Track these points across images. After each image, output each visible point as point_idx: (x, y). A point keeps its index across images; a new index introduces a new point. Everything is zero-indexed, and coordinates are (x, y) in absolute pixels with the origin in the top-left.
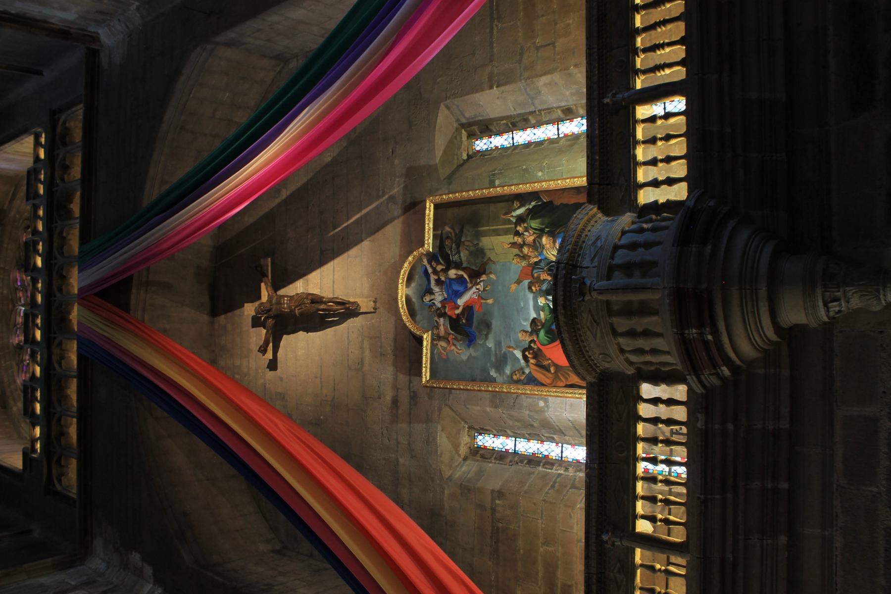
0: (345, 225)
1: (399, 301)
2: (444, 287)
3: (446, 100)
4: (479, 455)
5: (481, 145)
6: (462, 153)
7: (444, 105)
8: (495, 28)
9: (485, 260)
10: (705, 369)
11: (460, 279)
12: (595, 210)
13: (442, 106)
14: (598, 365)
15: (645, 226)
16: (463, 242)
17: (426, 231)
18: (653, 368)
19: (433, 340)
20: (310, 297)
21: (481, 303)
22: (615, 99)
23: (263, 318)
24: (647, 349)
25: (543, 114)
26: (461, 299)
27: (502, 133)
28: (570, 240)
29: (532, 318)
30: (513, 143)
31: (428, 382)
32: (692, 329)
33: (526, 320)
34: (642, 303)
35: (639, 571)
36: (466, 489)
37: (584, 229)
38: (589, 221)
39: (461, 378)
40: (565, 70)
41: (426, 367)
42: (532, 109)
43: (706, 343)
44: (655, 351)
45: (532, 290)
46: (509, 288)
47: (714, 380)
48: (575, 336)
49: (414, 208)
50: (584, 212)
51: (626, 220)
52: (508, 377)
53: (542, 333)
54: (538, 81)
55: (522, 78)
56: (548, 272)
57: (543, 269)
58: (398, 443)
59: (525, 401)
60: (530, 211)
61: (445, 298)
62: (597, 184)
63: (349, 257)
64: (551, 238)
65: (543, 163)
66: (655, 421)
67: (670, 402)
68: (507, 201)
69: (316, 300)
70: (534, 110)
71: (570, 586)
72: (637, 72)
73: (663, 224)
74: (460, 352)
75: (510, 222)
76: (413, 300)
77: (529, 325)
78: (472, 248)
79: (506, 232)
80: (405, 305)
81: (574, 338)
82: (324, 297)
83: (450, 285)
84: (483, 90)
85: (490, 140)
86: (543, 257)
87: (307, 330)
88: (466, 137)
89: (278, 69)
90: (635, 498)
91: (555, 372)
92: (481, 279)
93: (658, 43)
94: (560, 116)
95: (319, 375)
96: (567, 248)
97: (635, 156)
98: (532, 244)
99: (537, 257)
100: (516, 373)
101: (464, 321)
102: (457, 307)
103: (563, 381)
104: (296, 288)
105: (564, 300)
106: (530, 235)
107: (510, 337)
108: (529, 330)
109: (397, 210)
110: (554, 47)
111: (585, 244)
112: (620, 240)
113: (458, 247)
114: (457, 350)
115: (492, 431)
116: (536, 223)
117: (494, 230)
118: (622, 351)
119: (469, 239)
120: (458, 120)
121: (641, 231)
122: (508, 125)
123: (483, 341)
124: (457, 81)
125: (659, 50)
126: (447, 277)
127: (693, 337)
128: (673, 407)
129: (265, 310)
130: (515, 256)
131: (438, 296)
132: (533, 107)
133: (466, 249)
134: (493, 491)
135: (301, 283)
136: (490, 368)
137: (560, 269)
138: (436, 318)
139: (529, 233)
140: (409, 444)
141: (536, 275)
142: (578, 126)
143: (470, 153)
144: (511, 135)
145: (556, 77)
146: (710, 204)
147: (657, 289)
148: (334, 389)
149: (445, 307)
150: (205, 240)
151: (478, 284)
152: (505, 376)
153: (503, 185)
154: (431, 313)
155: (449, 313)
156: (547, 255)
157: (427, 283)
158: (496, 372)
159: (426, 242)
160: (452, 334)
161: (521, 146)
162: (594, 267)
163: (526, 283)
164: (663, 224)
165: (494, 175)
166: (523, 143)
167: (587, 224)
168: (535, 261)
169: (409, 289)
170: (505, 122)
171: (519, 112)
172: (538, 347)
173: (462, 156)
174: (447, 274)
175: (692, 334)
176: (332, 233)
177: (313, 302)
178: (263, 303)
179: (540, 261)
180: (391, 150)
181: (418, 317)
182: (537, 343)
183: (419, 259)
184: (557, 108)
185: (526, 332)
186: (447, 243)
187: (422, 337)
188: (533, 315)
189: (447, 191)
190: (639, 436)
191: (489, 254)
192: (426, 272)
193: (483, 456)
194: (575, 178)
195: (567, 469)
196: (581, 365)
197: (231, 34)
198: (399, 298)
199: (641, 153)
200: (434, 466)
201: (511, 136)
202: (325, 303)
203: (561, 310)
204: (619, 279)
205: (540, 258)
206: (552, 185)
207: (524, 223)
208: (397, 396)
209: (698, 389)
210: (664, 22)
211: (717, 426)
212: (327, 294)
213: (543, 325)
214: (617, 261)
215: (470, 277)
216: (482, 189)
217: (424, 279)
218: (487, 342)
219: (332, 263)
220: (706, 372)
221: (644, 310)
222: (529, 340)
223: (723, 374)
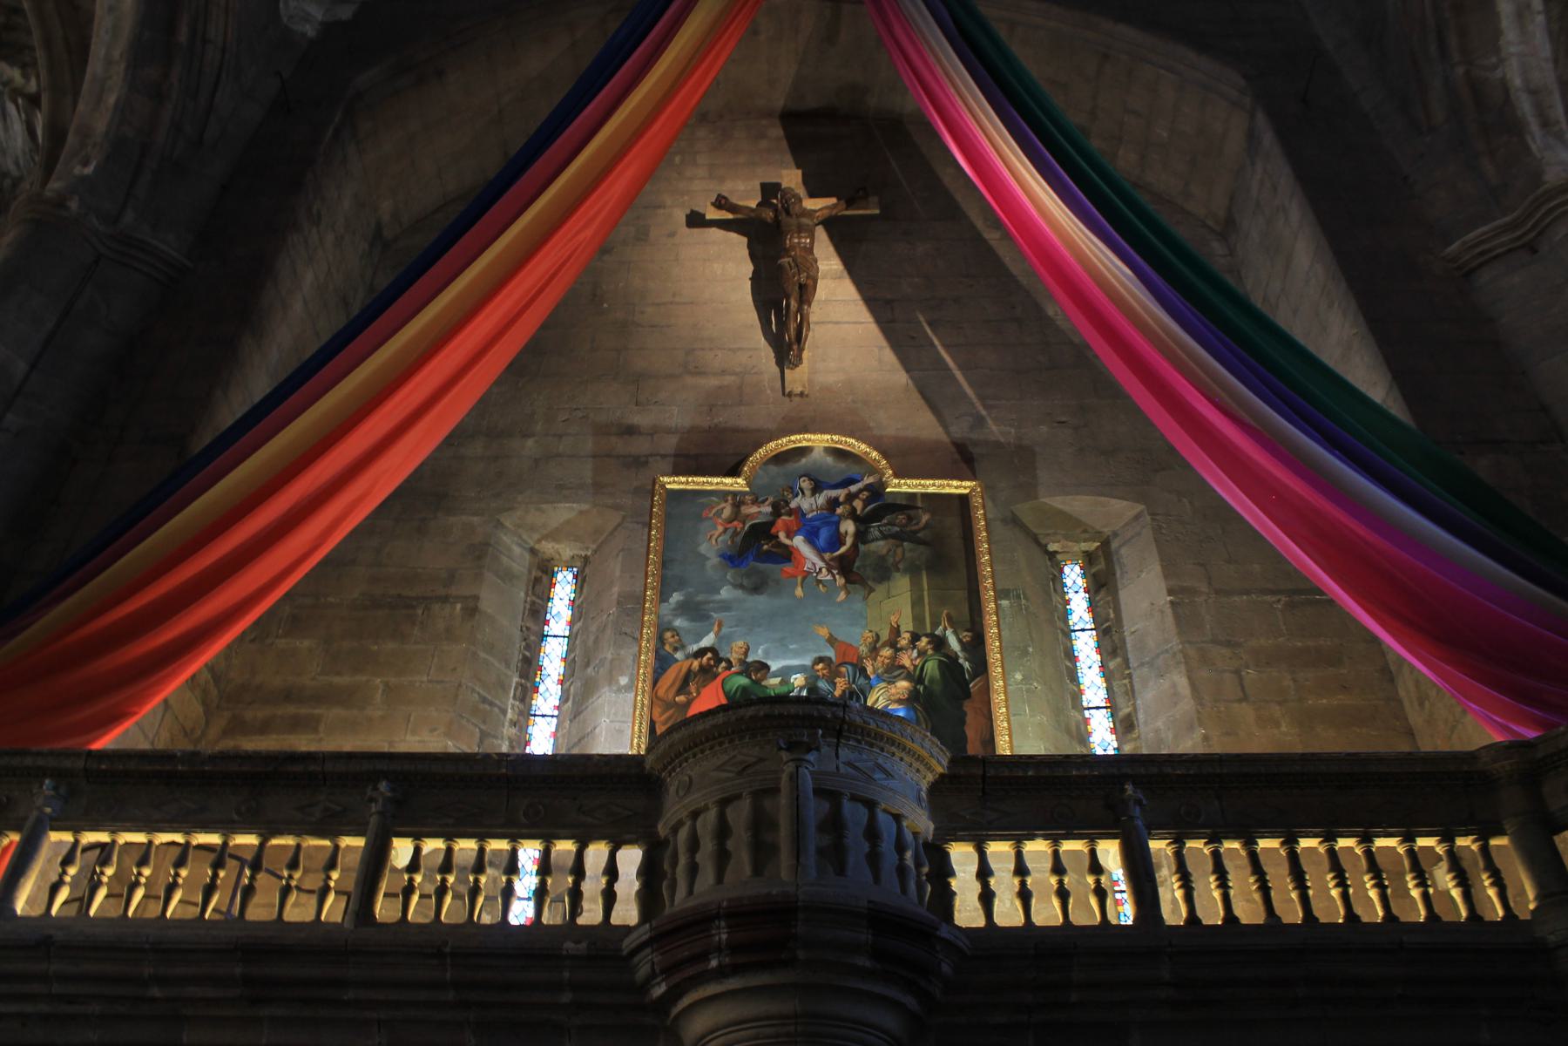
0: (936, 342)
1: (802, 436)
2: (825, 512)
3: (1150, 514)
4: (540, 574)
5: (1073, 576)
6: (1059, 542)
7: (1142, 512)
8: (1274, 599)
9: (870, 583)
10: (662, 954)
11: (838, 540)
12: (940, 770)
13: (1140, 507)
14: (673, 774)
15: (909, 855)
16: (902, 546)
17: (922, 482)
18: (666, 866)
19: (735, 494)
20: (810, 282)
21: (796, 577)
22: (1131, 803)
23: (775, 201)
24: (698, 858)
25: (1124, 681)
26: (804, 541)
27: (1092, 611)
28: (885, 727)
29: (769, 663)
30: (1075, 631)
31: (663, 486)
32: (727, 933)
33: (767, 653)
34: (774, 849)
35: (327, 843)
36: (480, 553)
37: (904, 749)
38: (919, 759)
39: (667, 542)
40: (1199, 719)
41: (687, 483)
42: (1133, 663)
43: (704, 957)
44: (693, 869)
45: (818, 664)
46: (821, 624)
47: (643, 972)
48: (720, 735)
49: (963, 459)
50: (935, 750)
51: (921, 822)
52: (670, 622)
53: (743, 681)
54: (1180, 672)
55: (1187, 645)
56: (847, 691)
57: (854, 682)
58: (560, 436)
59: (628, 653)
60: (953, 659)
61: (805, 515)
62: (984, 771)
63: (881, 348)
64: (906, 696)
65: (1038, 682)
66: (578, 871)
67: (609, 897)
68: (972, 621)
69: (806, 293)
70: (1131, 665)
71: (315, 730)
72: (1179, 841)
73: (912, 886)
74: (712, 541)
75: (935, 624)
76: (804, 461)
77: (757, 659)
78: (891, 560)
79: (918, 619)
80: (794, 446)
81: (716, 734)
82: (810, 306)
83: (828, 524)
84: (1166, 576)
85: (1082, 590)
86: (873, 682)
87: (755, 279)
88: (1087, 549)
89: (1210, 223)
90: (450, 837)
91: (676, 703)
92: (837, 577)
93: (1230, 877)
94: (1121, 709)
95: (677, 299)
96: (871, 721)
97: (1032, 838)
98: (896, 663)
99: (875, 671)
100: (677, 638)
101: (765, 547)
102: (790, 536)
103: (660, 716)
104: (828, 259)
105: (781, 716)
106: (912, 660)
107: (737, 626)
108: (750, 659)
109: (960, 430)
110: (1240, 701)
111: (878, 751)
112: (885, 811)
113: (894, 536)
114: (717, 533)
115: (580, 597)
116: (932, 669)
117: (921, 599)
118: (695, 815)
119: (908, 555)
120: (1115, 534)
121: (900, 848)
122: (1107, 620)
123: (732, 581)
124: (1182, 533)
125: (1217, 880)
126: (841, 517)
127: (713, 935)
128: (600, 901)
129: (788, 206)
130: (877, 635)
131: (808, 503)
132: (1136, 665)
133: (890, 550)
134: (476, 598)
135: (836, 267)
136: (683, 592)
137: (835, 709)
138: (771, 499)
139: (916, 659)
140: (559, 455)
141: (843, 669)
142: (1103, 739)
143: (1059, 557)
144: (1090, 628)
145: (1187, 705)
146: (943, 965)
147: (797, 873)
148: (652, 326)
149: (790, 515)
150: (912, 101)
151: (829, 571)
152: (670, 617)
153: (1001, 614)
154: (780, 490)
155: (779, 522)
156: (876, 690)
157: (833, 483)
158: (678, 602)
159: (903, 481)
160: (744, 527)
161: (1069, 644)
162: (837, 768)
163: (830, 653)
164: (912, 886)
165: (1018, 597)
166: (1075, 648)
167: (914, 755)
168: (868, 669)
169: (822, 453)
170: (1112, 616)
171: (1129, 640)
172: (719, 674)
173: (1053, 542)
174: (847, 518)
175: (720, 933)
176: (922, 319)
177: (802, 287)
178: (800, 200)
179: (867, 677)
180: (1064, 419)
181: (773, 469)
182: (727, 673)
183: (873, 469)
184: (1134, 706)
185: (746, 654)
186: (900, 517)
187: (739, 476)
189: (990, 516)
190: (553, 843)
191: (880, 590)
192: (852, 481)
193: (537, 581)
194: (1010, 736)
195: (514, 724)
196: (670, 746)
197: (1268, 139)
198: (806, 436)
199: (1037, 848)
200: (520, 498)
201: (1088, 627)
202: (800, 310)
203: (763, 710)
204: (815, 809)
205: (872, 677)
206: (998, 698)
207: (933, 649)
208: (640, 433)
209: (628, 944)
210: (1264, 889)
211: (566, 975)
212: (816, 312)
213: (757, 682)
214: (847, 806)
215: (841, 557)
216: (993, 578)
217: (839, 479)
218: (730, 587)
219: (871, 319)
220: (657, 958)
221: (762, 852)
222: (732, 659)
223: (653, 986)
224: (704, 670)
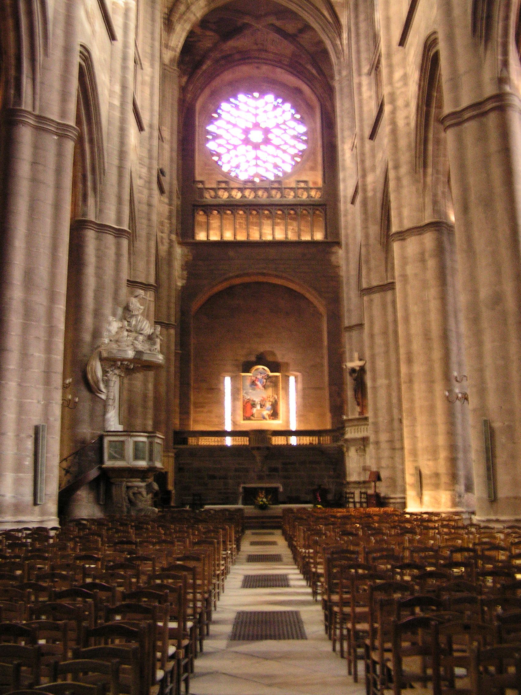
74: (248, 383)
131: (259, 377)
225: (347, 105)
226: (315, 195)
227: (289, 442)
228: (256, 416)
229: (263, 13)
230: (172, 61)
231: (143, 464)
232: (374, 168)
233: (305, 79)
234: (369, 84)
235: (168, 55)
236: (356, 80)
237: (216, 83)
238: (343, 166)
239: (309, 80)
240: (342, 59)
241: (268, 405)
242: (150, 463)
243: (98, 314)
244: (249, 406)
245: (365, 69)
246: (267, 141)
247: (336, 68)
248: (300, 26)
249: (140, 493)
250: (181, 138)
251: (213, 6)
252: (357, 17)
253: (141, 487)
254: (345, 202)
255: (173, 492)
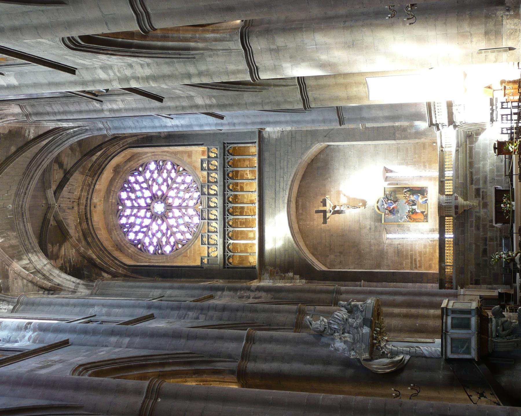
36: (390, 245)
59: (405, 226)
74: (392, 217)
79: (402, 194)
163: (407, 204)
188: (409, 209)
192: (382, 201)
224: (409, 217)
225: (129, 123)
226: (215, 152)
227: (451, 178)
228: (424, 210)
229: (44, 202)
230: (87, 287)
231: (474, 321)
232: (190, 98)
233: (106, 163)
234: (110, 101)
235: (83, 291)
236: (107, 114)
237: (108, 245)
238: (187, 126)
239: (108, 158)
240: (87, 128)
241: (413, 198)
242: (473, 313)
243: (327, 361)
244: (414, 216)
245: (97, 105)
246: (164, 198)
247: (96, 133)
248: (56, 167)
249: (503, 323)
250: (160, 279)
251: (38, 248)
252: (48, 114)
253: (497, 323)
254: (222, 125)
255: (500, 291)
